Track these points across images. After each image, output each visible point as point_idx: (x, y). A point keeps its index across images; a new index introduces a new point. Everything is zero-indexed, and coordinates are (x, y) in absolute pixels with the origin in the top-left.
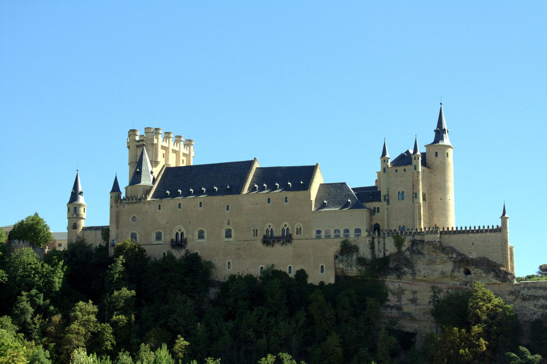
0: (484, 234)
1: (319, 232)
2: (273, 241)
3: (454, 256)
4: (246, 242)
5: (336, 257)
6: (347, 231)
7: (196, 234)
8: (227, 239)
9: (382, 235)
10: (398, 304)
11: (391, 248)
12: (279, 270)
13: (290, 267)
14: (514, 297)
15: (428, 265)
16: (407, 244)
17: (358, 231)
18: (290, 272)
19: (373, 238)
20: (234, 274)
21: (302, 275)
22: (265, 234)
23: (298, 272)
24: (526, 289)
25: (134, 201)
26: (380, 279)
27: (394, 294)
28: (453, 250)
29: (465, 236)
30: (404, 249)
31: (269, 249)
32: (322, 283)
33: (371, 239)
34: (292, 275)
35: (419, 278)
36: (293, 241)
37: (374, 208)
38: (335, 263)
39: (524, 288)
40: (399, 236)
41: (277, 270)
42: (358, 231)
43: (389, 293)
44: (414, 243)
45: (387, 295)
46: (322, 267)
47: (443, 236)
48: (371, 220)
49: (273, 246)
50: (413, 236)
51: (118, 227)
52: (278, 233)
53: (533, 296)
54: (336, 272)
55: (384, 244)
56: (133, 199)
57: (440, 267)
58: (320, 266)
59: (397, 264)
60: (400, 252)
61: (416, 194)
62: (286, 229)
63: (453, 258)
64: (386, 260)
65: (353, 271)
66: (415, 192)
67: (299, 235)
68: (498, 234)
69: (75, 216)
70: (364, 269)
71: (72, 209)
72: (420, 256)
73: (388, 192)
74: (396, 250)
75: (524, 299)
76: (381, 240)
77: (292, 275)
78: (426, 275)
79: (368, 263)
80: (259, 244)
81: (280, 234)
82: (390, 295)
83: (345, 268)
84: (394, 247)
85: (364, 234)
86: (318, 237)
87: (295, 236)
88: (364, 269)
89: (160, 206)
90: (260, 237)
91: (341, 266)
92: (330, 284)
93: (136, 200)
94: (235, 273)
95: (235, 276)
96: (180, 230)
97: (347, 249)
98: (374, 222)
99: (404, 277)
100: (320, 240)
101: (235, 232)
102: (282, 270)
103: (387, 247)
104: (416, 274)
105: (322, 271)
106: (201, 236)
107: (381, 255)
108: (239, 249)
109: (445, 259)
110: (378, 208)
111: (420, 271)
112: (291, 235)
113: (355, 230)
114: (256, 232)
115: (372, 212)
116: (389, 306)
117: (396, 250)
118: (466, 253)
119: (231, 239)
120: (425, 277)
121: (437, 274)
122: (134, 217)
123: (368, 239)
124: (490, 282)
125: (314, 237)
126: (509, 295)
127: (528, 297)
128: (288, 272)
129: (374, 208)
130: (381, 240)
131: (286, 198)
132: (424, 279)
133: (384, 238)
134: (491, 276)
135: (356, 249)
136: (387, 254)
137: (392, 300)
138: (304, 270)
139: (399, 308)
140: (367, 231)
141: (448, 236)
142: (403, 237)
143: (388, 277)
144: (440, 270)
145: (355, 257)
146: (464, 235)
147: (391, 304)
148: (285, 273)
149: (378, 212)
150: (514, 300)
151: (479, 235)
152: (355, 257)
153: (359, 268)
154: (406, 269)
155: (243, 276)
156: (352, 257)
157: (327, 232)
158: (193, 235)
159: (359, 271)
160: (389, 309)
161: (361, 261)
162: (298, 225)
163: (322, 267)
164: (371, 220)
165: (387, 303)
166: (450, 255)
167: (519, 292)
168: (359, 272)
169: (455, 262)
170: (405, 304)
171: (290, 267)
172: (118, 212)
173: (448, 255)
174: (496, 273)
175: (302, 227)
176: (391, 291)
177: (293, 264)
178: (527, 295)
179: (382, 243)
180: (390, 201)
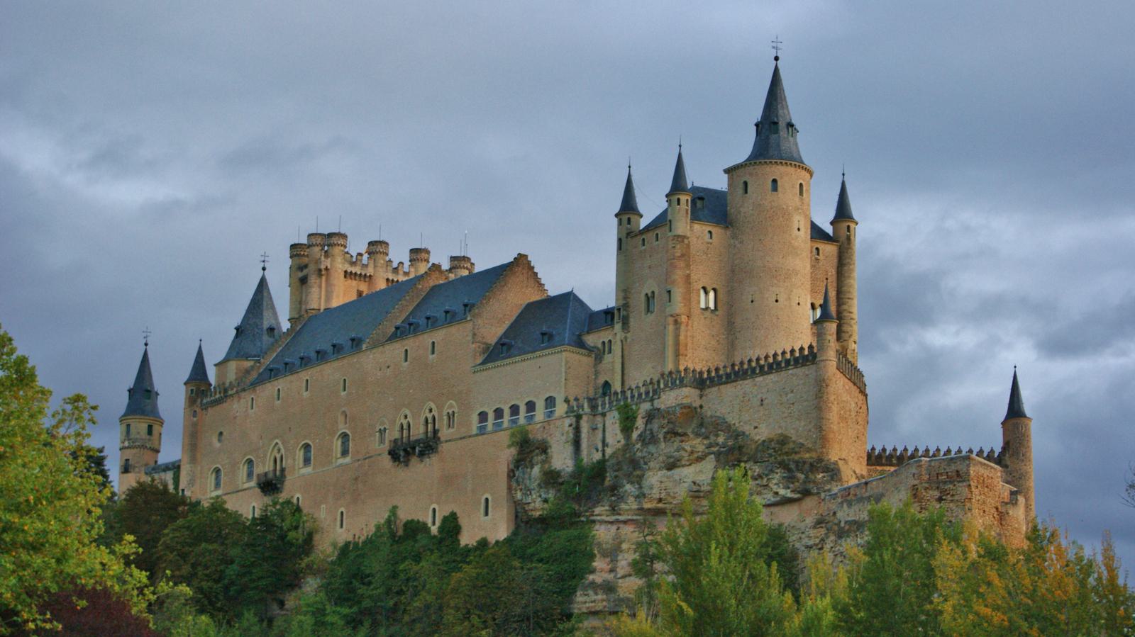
0: (783, 373)
1: (483, 416)
2: (405, 450)
3: (721, 440)
4: (367, 460)
5: (511, 475)
6: (531, 406)
7: (300, 454)
8: (341, 461)
9: (600, 408)
10: (610, 577)
11: (615, 437)
12: (416, 519)
13: (434, 510)
14: (823, 531)
15: (671, 466)
16: (640, 423)
17: (550, 402)
18: (434, 523)
19: (579, 417)
20: (348, 540)
21: (451, 526)
22: (397, 435)
23: (445, 519)
24: (845, 505)
25: (218, 396)
26: (583, 519)
27: (605, 554)
28: (720, 425)
29: (746, 385)
30: (635, 435)
31: (402, 474)
32: (483, 543)
33: (574, 419)
34: (434, 530)
35: (647, 506)
36: (440, 448)
37: (604, 343)
38: (510, 488)
39: (842, 503)
40: (626, 406)
41: (412, 521)
42: (550, 402)
43: (596, 552)
44: (650, 417)
45: (592, 557)
46: (487, 500)
47: (707, 391)
48: (597, 373)
49: (407, 464)
50: (652, 400)
51: (193, 460)
52: (418, 432)
53: (855, 522)
54: (517, 512)
55: (604, 431)
56: (215, 394)
57: (688, 474)
58: (483, 501)
59: (616, 477)
60: (628, 446)
61: (669, 292)
62: (430, 416)
63: (717, 444)
64: (599, 470)
65: (537, 504)
66: (669, 287)
67: (451, 430)
68: (808, 370)
69: (126, 444)
70: (551, 495)
71: (124, 427)
72: (652, 448)
73: (625, 298)
74: (623, 442)
75: (841, 534)
76: (599, 419)
77: (434, 530)
78: (662, 496)
79: (560, 480)
80: (386, 461)
81: (422, 429)
82: (598, 556)
83: (524, 501)
84: (618, 432)
85: (561, 408)
86: (482, 431)
87: (445, 433)
88: (551, 495)
89: (252, 399)
90: (387, 446)
91: (519, 495)
92: (497, 542)
93: (220, 393)
94: (350, 538)
95: (350, 542)
96: (279, 450)
97: (528, 449)
98: (601, 381)
99: (623, 506)
100: (485, 436)
101: (353, 440)
102: (421, 520)
103: (609, 440)
104: (644, 495)
105: (486, 514)
106: (307, 461)
107: (597, 456)
108: (356, 479)
109: (701, 448)
110: (610, 341)
111: (651, 488)
112: (438, 430)
113: (546, 400)
114: (382, 432)
115: (598, 354)
116: (593, 585)
117: (623, 442)
118: (747, 429)
119: (348, 460)
120: (660, 500)
121: (682, 492)
122: (221, 434)
123: (567, 422)
124: (778, 499)
125: (475, 431)
126: (815, 527)
127: (847, 527)
128: (430, 525)
129: (604, 343)
130: (599, 419)
131: (433, 343)
132: (660, 505)
133: (604, 415)
134: (775, 481)
135: (544, 448)
136: (609, 451)
137: (600, 569)
138: (455, 514)
139: (609, 588)
140: (567, 401)
141: (715, 389)
142: (634, 407)
143: (598, 510)
144: (689, 481)
145: (536, 471)
146: (746, 382)
147: (597, 578)
148: (425, 524)
149: (610, 352)
150: (823, 540)
151: (772, 377)
152: (536, 471)
153: (543, 496)
154: (628, 487)
155: (361, 541)
156: (532, 468)
157: (499, 413)
158: (294, 460)
159: (546, 501)
160: (591, 592)
161: (551, 478)
162: (452, 405)
163: (487, 500)
164: (597, 373)
165: (591, 577)
166: (712, 438)
167: (835, 513)
168: (546, 506)
169: (718, 455)
170: (623, 577)
171: (434, 510)
172: (195, 425)
173: (707, 438)
174: (789, 470)
175: (456, 411)
176: (599, 544)
177: (438, 504)
178: (846, 522)
179: (600, 426)
180: (632, 320)
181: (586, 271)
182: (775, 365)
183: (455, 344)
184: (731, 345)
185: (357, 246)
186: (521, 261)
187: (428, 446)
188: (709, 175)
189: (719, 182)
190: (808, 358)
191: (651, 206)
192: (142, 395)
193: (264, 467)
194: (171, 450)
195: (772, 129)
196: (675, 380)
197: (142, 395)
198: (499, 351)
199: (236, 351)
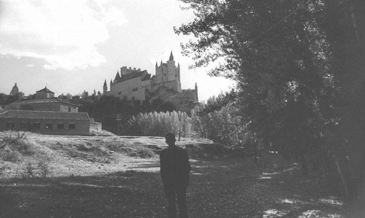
31: (134, 93)
97: (147, 90)
181: (152, 72)
182: (171, 81)
183: (139, 78)
184: (167, 79)
185: (128, 68)
186: (146, 71)
187: (136, 89)
188: (165, 62)
189: (166, 63)
190: (175, 81)
191: (159, 65)
192: (105, 84)
193: (119, 92)
194: (109, 90)
195: (171, 58)
196: (161, 83)
197: (105, 84)
198: (143, 80)
199: (115, 80)
